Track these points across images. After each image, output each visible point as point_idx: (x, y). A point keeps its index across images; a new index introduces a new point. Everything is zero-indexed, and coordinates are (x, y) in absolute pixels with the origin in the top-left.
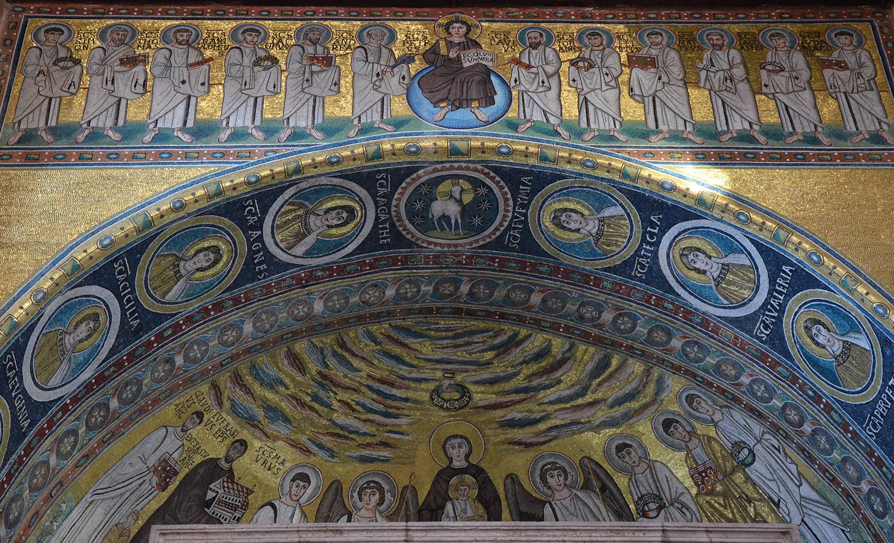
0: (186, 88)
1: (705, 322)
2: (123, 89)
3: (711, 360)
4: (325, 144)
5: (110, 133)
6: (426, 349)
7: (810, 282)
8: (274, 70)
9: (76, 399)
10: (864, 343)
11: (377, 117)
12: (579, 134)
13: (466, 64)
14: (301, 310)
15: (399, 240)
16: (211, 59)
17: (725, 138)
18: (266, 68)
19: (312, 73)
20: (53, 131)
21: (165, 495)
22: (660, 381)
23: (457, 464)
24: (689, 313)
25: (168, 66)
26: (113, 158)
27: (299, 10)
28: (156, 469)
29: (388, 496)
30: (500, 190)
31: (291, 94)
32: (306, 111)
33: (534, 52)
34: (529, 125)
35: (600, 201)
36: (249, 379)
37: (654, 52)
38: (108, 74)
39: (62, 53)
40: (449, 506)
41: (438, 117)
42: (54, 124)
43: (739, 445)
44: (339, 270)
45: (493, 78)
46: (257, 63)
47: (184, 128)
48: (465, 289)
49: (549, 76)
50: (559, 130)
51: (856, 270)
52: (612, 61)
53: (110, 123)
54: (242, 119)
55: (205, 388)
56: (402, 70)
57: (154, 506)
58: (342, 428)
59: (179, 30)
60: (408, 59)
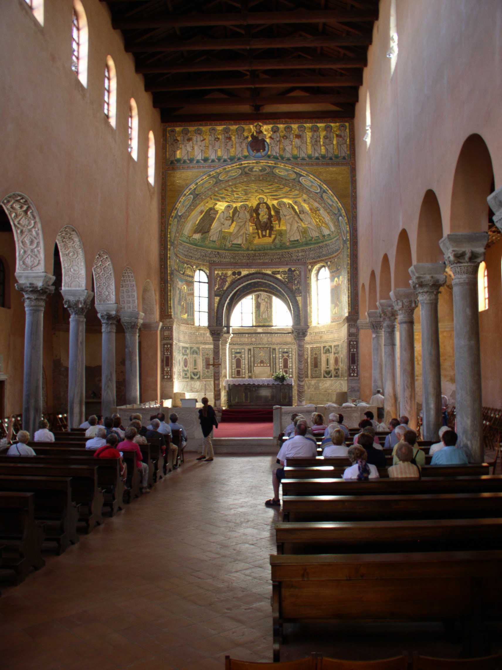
0: (201, 148)
1: (309, 190)
2: (189, 149)
3: (311, 195)
4: (230, 163)
5: (187, 161)
6: (253, 184)
7: (326, 193)
8: (219, 142)
9: (186, 210)
10: (334, 205)
11: (241, 156)
12: (283, 158)
13: (260, 138)
14: (227, 184)
15: (246, 173)
16: (205, 139)
17: (313, 159)
18: (217, 141)
19: (227, 142)
20: (176, 160)
21: (202, 216)
22: (302, 195)
23: (261, 202)
24: (306, 188)
25: (197, 142)
26: (188, 168)
27: (223, 123)
28: (200, 212)
29: (247, 208)
30: (267, 168)
31: (223, 149)
32: (226, 154)
33: (275, 134)
34: (272, 157)
35: (287, 170)
36: (217, 195)
37: (301, 133)
38: (185, 144)
39: (175, 138)
40: (260, 209)
41: (253, 155)
42: (176, 159)
43: (317, 207)
44: (235, 179)
45: (266, 143)
46: (215, 140)
47: (202, 160)
48: (261, 178)
49: (278, 142)
50: (280, 158)
51: (334, 194)
52: (291, 137)
53: (187, 159)
54: (213, 157)
55: (209, 199)
56: (246, 141)
57: (199, 218)
58: (237, 197)
59: (198, 130)
60: (247, 137)
